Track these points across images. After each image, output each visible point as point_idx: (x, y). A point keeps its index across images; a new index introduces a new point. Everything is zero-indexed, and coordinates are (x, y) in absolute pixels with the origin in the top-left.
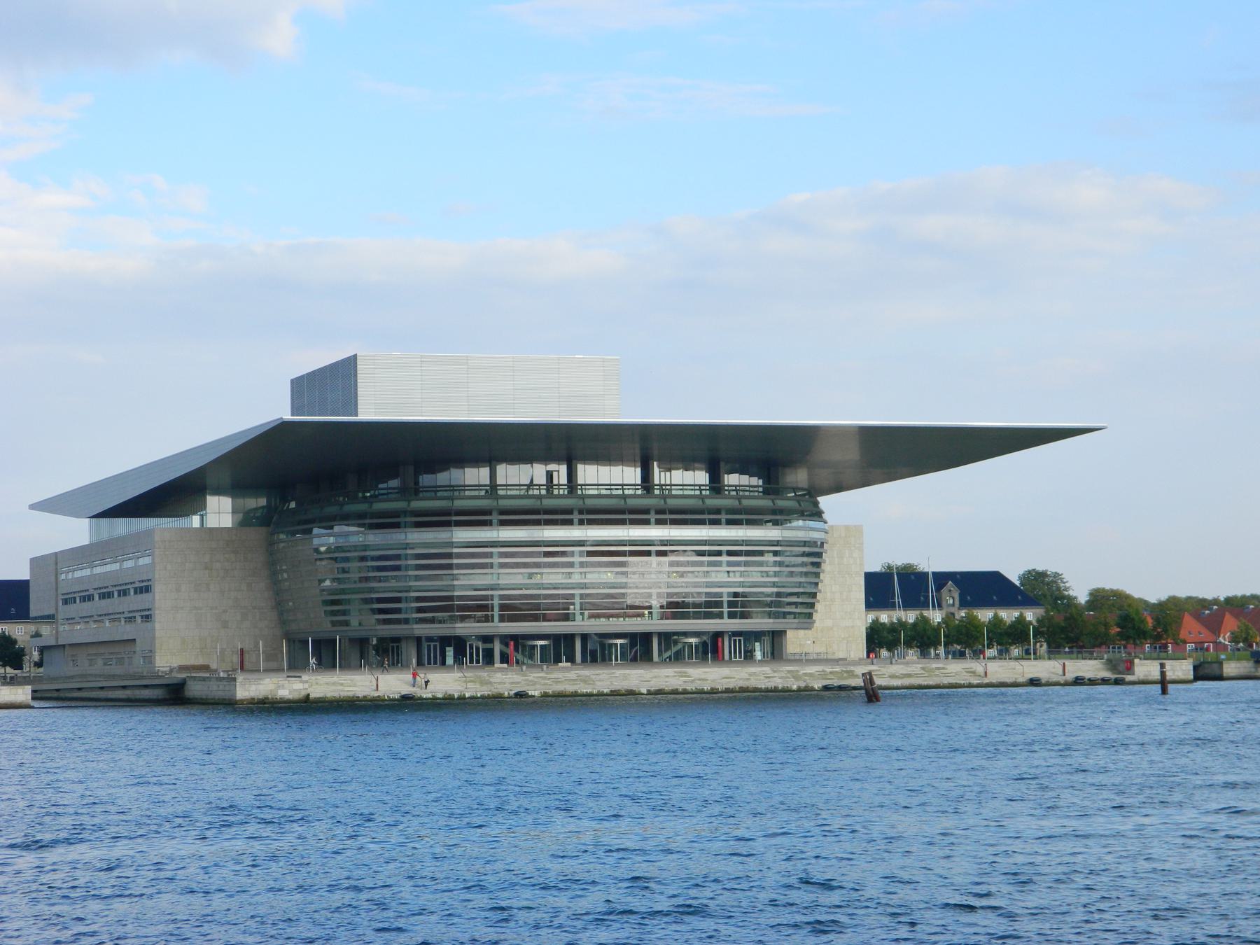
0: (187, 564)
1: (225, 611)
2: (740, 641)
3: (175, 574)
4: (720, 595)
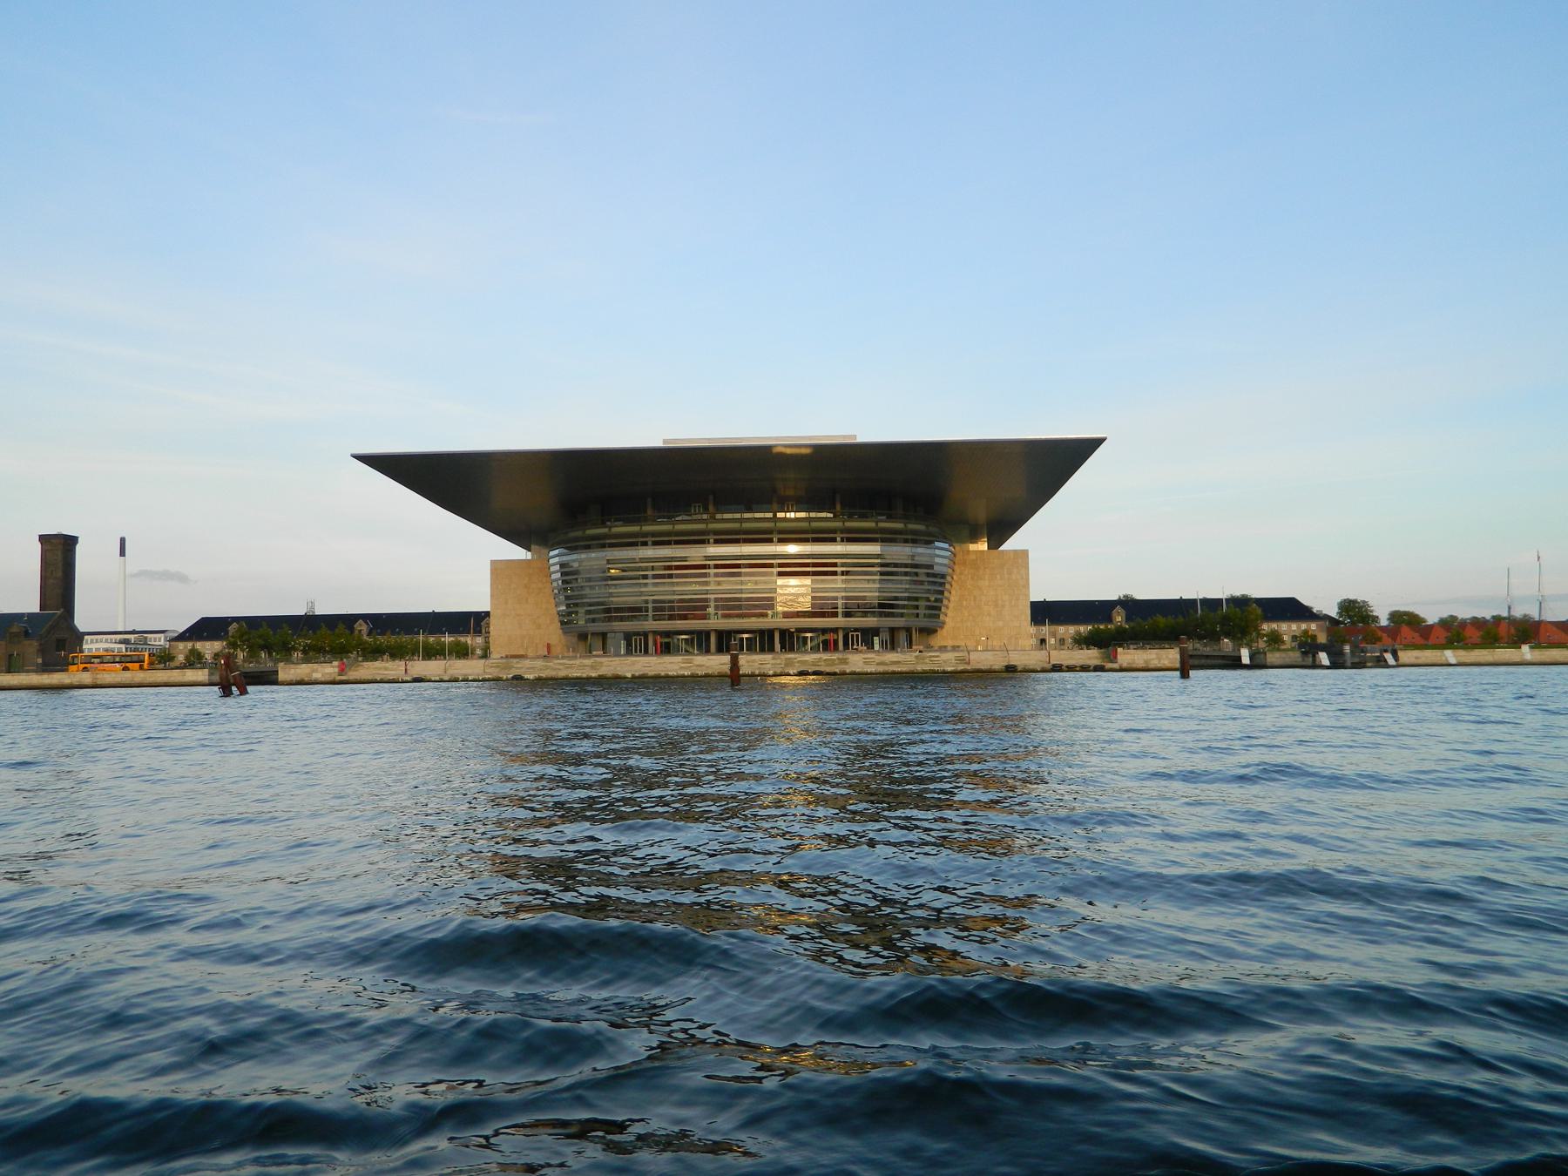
1: (538, 617)
2: (857, 636)
4: (836, 598)
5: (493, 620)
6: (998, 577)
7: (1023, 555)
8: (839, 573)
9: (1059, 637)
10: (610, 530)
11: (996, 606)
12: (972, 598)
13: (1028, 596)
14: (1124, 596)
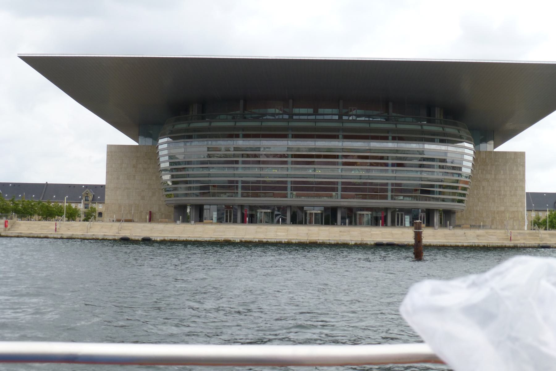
0: (123, 165)
1: (143, 191)
2: (402, 215)
3: (117, 170)
4: (387, 184)
5: (108, 193)
6: (502, 172)
8: (390, 164)
10: (210, 124)
11: (500, 195)
12: (481, 189)
13: (523, 188)
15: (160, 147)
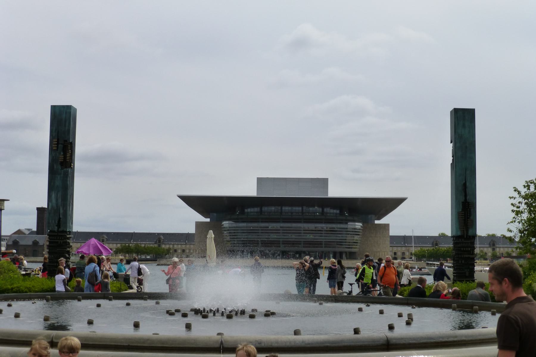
4: (322, 242)
7: (386, 227)
9: (410, 252)
14: (441, 234)
15: (224, 225)
